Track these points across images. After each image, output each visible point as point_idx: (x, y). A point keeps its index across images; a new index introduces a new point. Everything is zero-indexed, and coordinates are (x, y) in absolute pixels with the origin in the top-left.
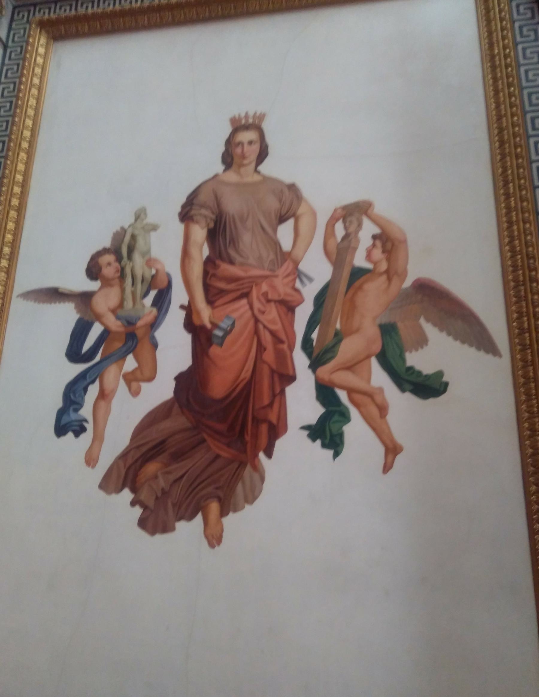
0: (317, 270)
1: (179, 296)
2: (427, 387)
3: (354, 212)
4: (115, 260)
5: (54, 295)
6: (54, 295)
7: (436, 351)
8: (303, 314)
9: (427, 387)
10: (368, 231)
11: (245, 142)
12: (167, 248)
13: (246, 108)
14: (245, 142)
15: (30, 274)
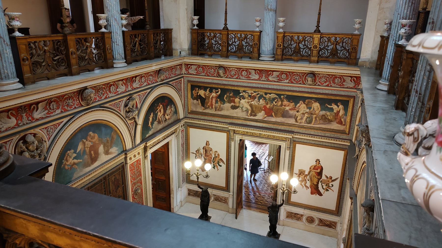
0: (213, 156)
1: (203, 155)
2: (221, 166)
3: (216, 152)
4: (198, 151)
5: (193, 153)
6: (193, 153)
7: (221, 164)
8: (212, 159)
9: (221, 166)
10: (217, 154)
11: (207, 143)
12: (202, 151)
13: (208, 140)
14: (207, 143)
15: (191, 151)
